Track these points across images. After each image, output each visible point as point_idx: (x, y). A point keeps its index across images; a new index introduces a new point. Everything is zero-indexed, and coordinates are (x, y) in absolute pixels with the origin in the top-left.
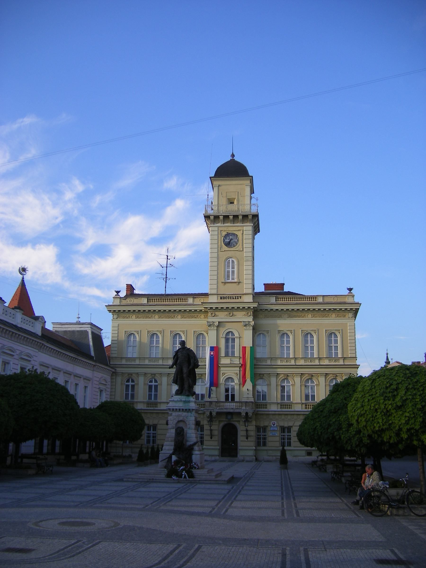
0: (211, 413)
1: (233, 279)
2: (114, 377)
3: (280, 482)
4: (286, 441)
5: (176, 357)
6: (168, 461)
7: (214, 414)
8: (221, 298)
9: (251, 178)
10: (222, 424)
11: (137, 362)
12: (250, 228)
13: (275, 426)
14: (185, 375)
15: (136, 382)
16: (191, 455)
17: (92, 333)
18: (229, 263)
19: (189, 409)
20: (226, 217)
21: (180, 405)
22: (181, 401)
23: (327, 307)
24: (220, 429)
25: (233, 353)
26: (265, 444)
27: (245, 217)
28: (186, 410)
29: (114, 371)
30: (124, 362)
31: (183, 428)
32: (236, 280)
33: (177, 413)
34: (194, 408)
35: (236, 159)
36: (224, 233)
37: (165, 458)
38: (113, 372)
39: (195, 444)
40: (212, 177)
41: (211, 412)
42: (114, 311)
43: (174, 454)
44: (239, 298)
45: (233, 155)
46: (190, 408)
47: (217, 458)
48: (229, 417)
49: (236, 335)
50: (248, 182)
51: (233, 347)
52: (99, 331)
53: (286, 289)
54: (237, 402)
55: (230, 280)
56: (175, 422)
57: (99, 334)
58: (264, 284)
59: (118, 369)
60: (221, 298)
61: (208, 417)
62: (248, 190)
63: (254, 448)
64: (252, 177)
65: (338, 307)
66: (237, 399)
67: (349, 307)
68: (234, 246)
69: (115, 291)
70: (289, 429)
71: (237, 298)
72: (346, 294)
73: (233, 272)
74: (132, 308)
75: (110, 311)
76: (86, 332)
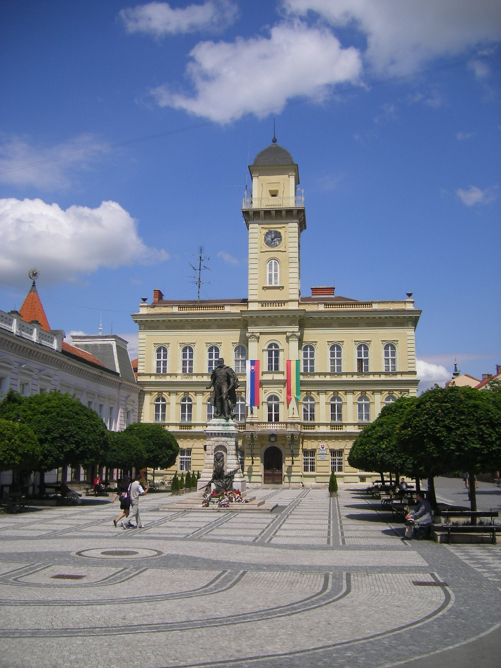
0: (252, 436)
3: (328, 510)
4: (337, 465)
8: (262, 306)
10: (264, 448)
12: (296, 225)
13: (324, 449)
18: (271, 265)
20: (267, 213)
22: (219, 425)
24: (263, 453)
25: (277, 368)
26: (313, 469)
32: (278, 285)
35: (279, 144)
39: (235, 471)
40: (251, 166)
44: (283, 304)
45: (275, 141)
48: (273, 439)
49: (280, 348)
51: (277, 361)
52: (124, 344)
53: (337, 293)
54: (281, 423)
55: (273, 285)
56: (214, 447)
60: (262, 306)
62: (292, 180)
66: (281, 420)
68: (277, 246)
70: (340, 452)
71: (280, 305)
73: (276, 275)
75: (136, 322)
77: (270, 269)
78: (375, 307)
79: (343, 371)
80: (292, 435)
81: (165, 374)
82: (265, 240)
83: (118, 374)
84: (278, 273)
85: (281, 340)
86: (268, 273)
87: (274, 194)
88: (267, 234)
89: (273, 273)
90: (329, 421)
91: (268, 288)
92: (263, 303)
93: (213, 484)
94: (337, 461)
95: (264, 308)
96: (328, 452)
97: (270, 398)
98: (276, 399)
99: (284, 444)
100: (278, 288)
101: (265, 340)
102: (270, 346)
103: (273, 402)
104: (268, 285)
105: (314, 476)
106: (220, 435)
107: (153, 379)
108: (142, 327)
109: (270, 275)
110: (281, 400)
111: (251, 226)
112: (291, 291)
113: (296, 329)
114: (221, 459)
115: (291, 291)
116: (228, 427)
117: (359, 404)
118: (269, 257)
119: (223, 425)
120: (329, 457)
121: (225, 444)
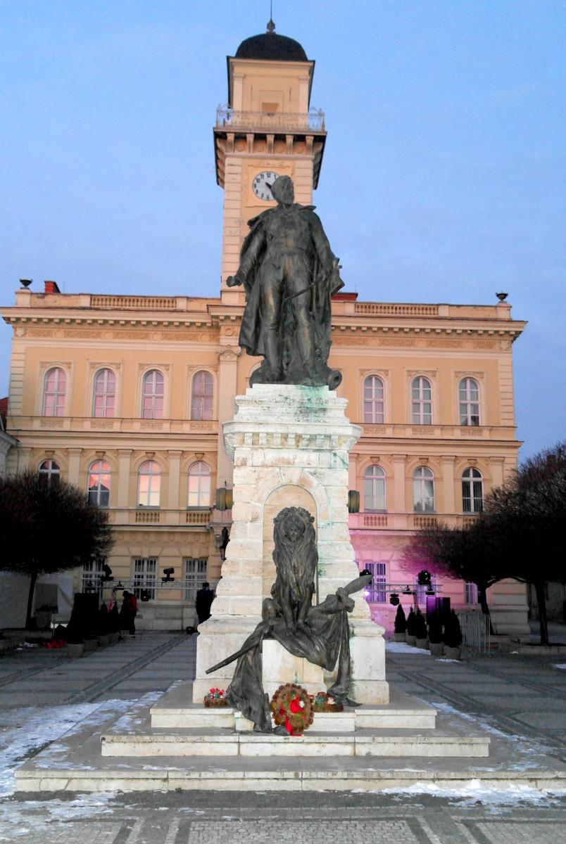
2: (14, 457)
9: (312, 64)
11: (67, 426)
15: (62, 468)
20: (260, 138)
23: (459, 326)
27: (299, 138)
29: (14, 442)
30: (37, 425)
31: (309, 515)
37: (223, 658)
38: (12, 447)
40: (233, 58)
41: (225, 528)
42: (18, 319)
43: (269, 636)
45: (271, 25)
50: (306, 73)
59: (24, 442)
61: (217, 540)
64: (314, 62)
65: (480, 327)
67: (502, 328)
69: (22, 281)
72: (495, 305)
74: (57, 315)
75: (8, 320)
108: (20, 332)
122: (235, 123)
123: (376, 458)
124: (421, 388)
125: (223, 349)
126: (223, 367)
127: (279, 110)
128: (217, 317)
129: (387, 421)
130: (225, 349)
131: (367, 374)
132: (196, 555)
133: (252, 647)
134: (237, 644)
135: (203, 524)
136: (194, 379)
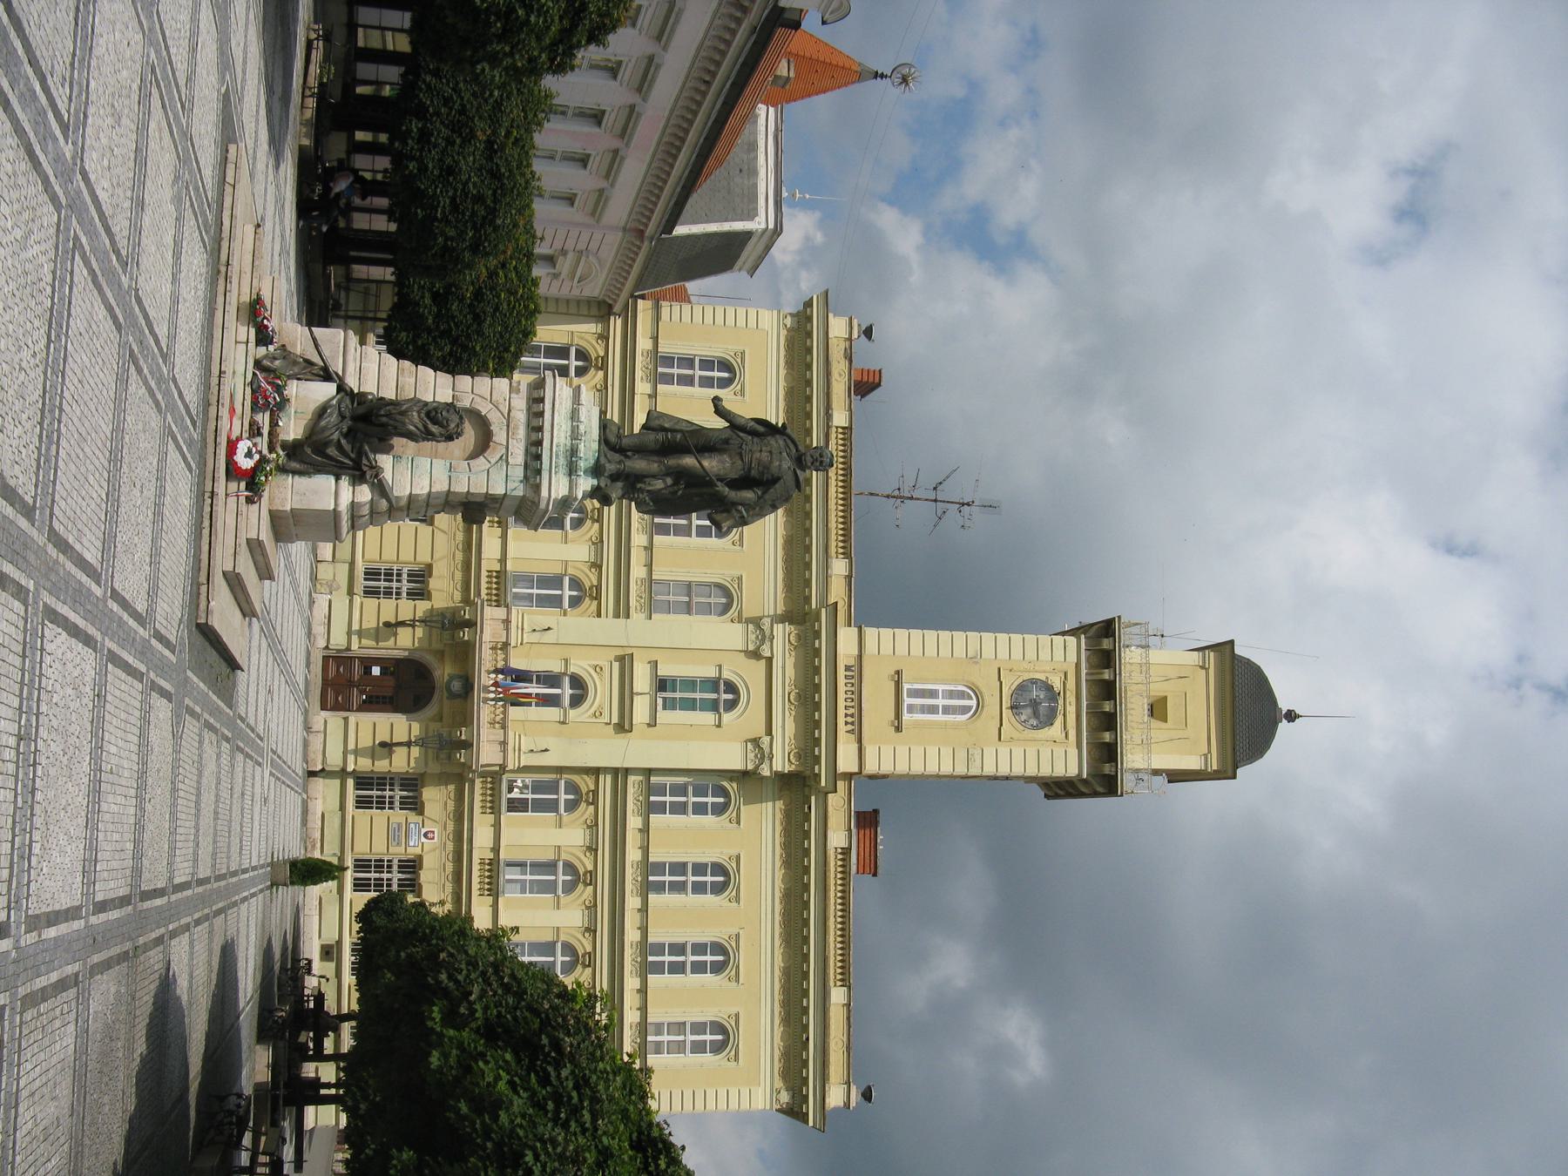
0: (471, 624)
1: (911, 709)
2: (594, 311)
3: (203, 873)
5: (761, 429)
6: (309, 363)
7: (466, 635)
8: (848, 668)
9: (1230, 773)
12: (1073, 771)
14: (689, 461)
16: (337, 470)
17: (747, 236)
18: (962, 695)
19: (539, 472)
20: (1107, 690)
21: (558, 434)
22: (575, 435)
25: (670, 705)
26: (362, 803)
28: (538, 457)
32: (906, 717)
33: (520, 416)
34: (544, 493)
35: (1283, 726)
36: (1057, 684)
37: (326, 352)
38: (610, 307)
39: (381, 489)
42: (810, 319)
44: (850, 727)
45: (1291, 716)
46: (545, 475)
47: (322, 643)
49: (727, 717)
55: (907, 701)
56: (484, 408)
57: (737, 267)
58: (876, 812)
60: (848, 668)
62: (1193, 763)
63: (350, 768)
71: (849, 719)
73: (933, 710)
76: (751, 214)
77: (951, 694)
78: (838, 995)
79: (652, 897)
80: (467, 745)
81: (657, 379)
82: (1034, 681)
83: (669, 227)
84: (940, 717)
85: (747, 718)
86: (940, 688)
87: (1157, 709)
88: (1049, 688)
89: (940, 702)
90: (504, 855)
91: (898, 685)
92: (857, 670)
93: (329, 389)
94: (385, 876)
95: (841, 673)
96: (414, 851)
97: (577, 682)
98: (577, 701)
99: (441, 720)
100: (898, 715)
101: (749, 675)
102: (731, 687)
103: (567, 692)
104: (906, 687)
105: (342, 808)
106: (534, 437)
107: (643, 343)
109: (933, 694)
110: (572, 713)
111: (1072, 640)
112: (887, 752)
113: (781, 762)
114: (434, 429)
115: (887, 752)
116: (563, 470)
117: (554, 943)
118: (984, 690)
119: (573, 452)
120: (398, 852)
121: (494, 454)
122: (1130, 657)
123: (591, 879)
124: (709, 958)
125: (766, 627)
126: (739, 627)
127: (1155, 723)
128: (818, 619)
129: (652, 897)
130: (767, 633)
131: (731, 867)
132: (433, 583)
133: (326, 375)
134: (336, 366)
135: (484, 592)
136: (719, 586)
